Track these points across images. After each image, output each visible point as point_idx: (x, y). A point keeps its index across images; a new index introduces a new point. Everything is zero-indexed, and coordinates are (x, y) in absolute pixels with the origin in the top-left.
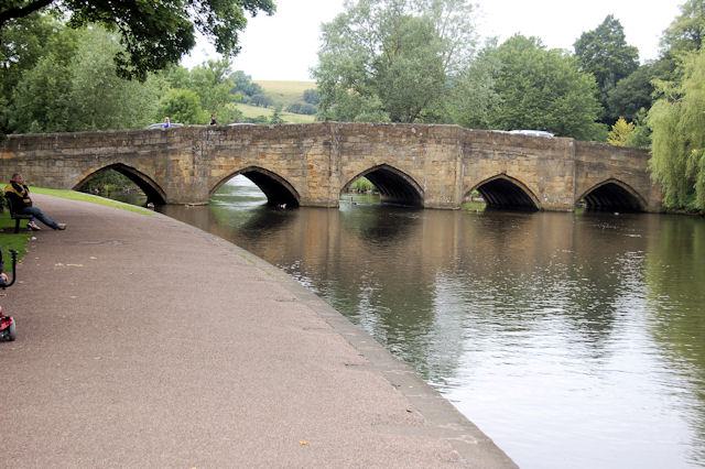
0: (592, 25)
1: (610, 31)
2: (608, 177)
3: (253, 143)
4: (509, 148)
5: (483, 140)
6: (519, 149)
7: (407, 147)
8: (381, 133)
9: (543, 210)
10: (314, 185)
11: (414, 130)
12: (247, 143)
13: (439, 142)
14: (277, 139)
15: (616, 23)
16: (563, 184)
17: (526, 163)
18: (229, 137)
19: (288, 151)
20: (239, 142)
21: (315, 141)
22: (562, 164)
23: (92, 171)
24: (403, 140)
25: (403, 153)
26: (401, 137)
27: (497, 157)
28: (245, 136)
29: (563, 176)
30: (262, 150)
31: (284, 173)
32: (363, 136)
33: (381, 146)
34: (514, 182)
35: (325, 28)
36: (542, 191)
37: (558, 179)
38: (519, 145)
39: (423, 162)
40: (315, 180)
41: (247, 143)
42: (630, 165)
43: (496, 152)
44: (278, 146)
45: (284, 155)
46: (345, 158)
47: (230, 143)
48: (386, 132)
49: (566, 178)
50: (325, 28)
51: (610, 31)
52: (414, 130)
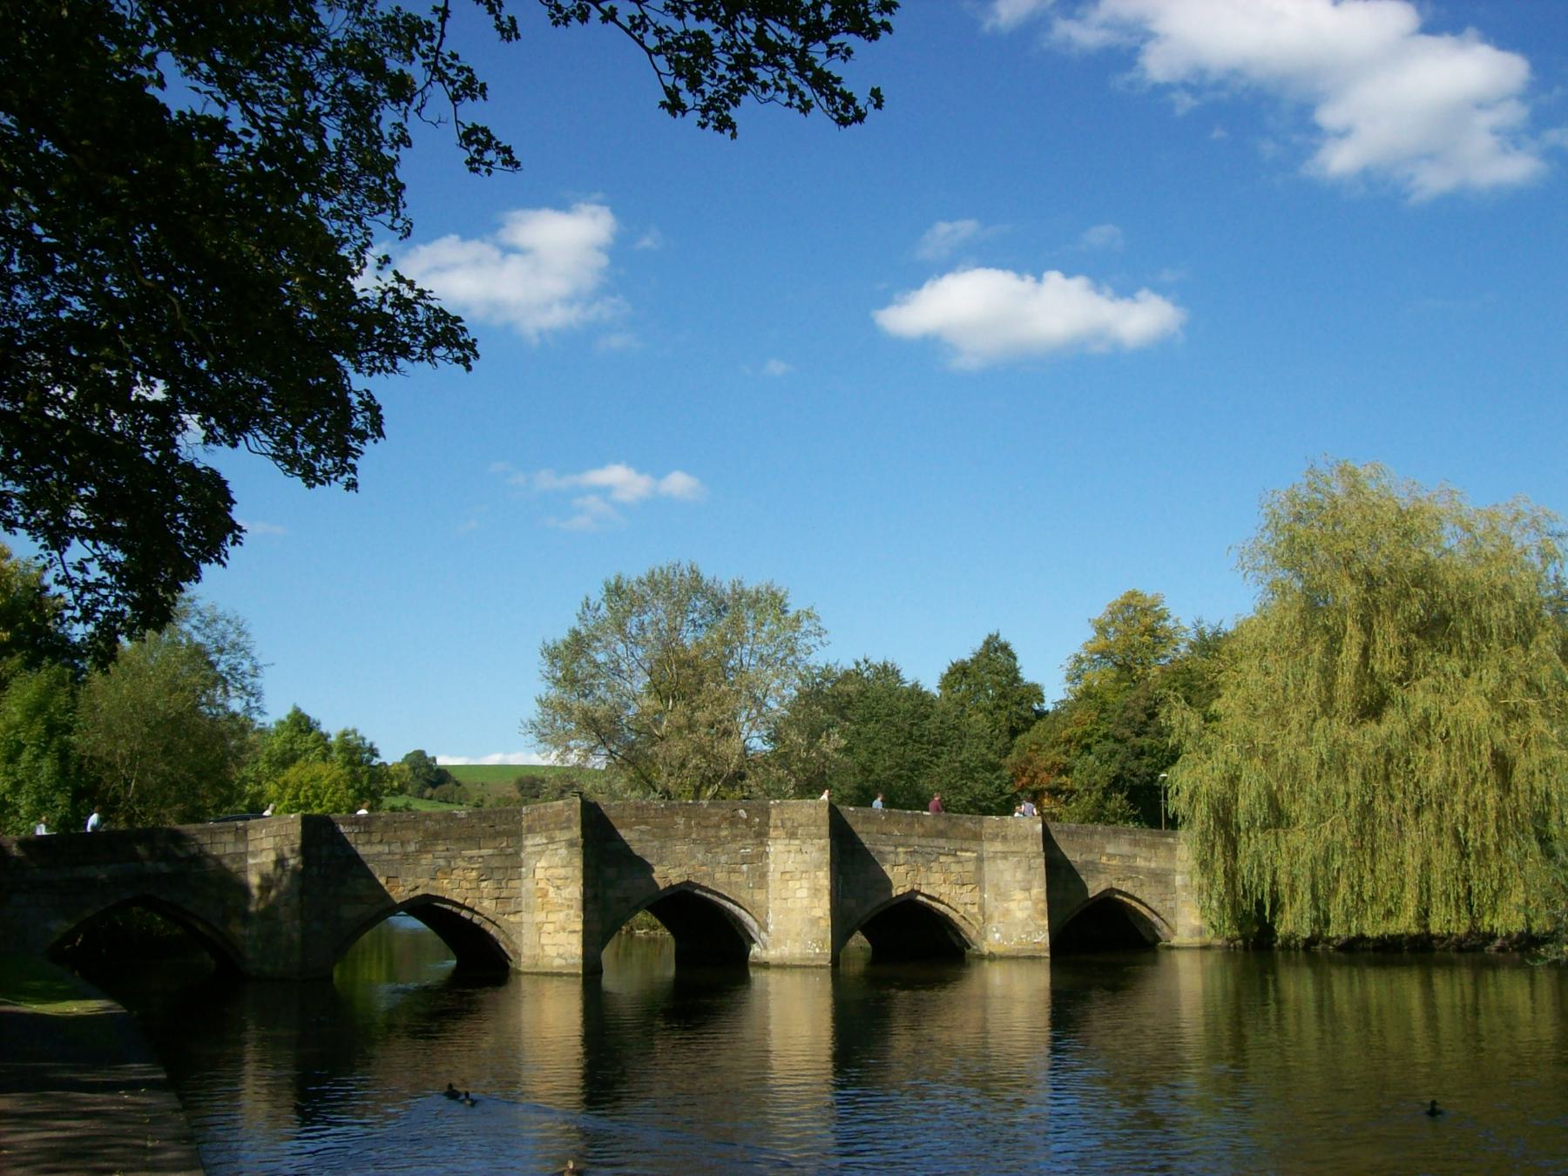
0: (966, 649)
1: (996, 655)
2: (1103, 887)
3: (423, 849)
4: (923, 842)
5: (875, 828)
6: (942, 842)
7: (734, 846)
8: (681, 821)
9: (992, 957)
10: (549, 928)
11: (742, 813)
12: (412, 848)
13: (792, 835)
14: (474, 840)
15: (1005, 648)
16: (1029, 903)
17: (955, 868)
18: (376, 837)
19: (495, 863)
20: (396, 848)
21: (552, 841)
22: (1024, 865)
23: (89, 913)
24: (724, 833)
25: (723, 859)
26: (718, 826)
27: (901, 859)
28: (410, 834)
29: (1028, 890)
30: (442, 862)
31: (488, 905)
32: (643, 827)
33: (681, 848)
34: (934, 904)
35: (553, 655)
37: (1019, 895)
38: (941, 834)
39: (763, 875)
40: (552, 917)
41: (412, 848)
42: (1140, 862)
43: (900, 850)
44: (475, 852)
45: (487, 873)
46: (611, 872)
47: (379, 848)
48: (689, 818)
49: (1035, 891)
50: (553, 655)
51: (996, 655)
52: (742, 813)
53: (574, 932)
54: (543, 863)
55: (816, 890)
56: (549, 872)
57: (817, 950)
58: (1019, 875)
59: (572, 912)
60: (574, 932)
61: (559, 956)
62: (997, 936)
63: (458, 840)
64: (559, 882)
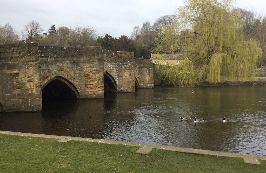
20: (49, 59)
36: (140, 81)
37: (147, 76)
41: (53, 59)
49: (151, 75)
53: (101, 87)
54: (88, 65)
55: (131, 74)
56: (90, 69)
57: (131, 89)
58: (147, 72)
59: (100, 81)
60: (101, 87)
61: (95, 95)
62: (142, 84)
63: (64, 57)
64: (94, 72)
